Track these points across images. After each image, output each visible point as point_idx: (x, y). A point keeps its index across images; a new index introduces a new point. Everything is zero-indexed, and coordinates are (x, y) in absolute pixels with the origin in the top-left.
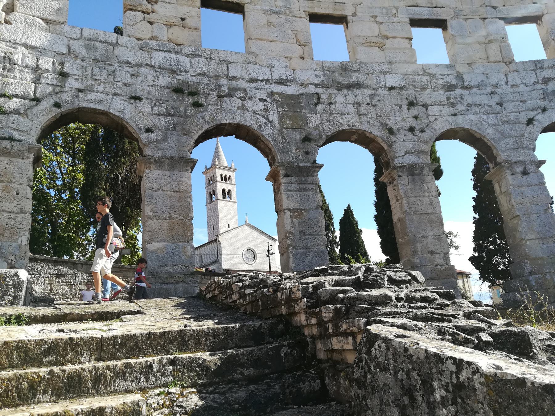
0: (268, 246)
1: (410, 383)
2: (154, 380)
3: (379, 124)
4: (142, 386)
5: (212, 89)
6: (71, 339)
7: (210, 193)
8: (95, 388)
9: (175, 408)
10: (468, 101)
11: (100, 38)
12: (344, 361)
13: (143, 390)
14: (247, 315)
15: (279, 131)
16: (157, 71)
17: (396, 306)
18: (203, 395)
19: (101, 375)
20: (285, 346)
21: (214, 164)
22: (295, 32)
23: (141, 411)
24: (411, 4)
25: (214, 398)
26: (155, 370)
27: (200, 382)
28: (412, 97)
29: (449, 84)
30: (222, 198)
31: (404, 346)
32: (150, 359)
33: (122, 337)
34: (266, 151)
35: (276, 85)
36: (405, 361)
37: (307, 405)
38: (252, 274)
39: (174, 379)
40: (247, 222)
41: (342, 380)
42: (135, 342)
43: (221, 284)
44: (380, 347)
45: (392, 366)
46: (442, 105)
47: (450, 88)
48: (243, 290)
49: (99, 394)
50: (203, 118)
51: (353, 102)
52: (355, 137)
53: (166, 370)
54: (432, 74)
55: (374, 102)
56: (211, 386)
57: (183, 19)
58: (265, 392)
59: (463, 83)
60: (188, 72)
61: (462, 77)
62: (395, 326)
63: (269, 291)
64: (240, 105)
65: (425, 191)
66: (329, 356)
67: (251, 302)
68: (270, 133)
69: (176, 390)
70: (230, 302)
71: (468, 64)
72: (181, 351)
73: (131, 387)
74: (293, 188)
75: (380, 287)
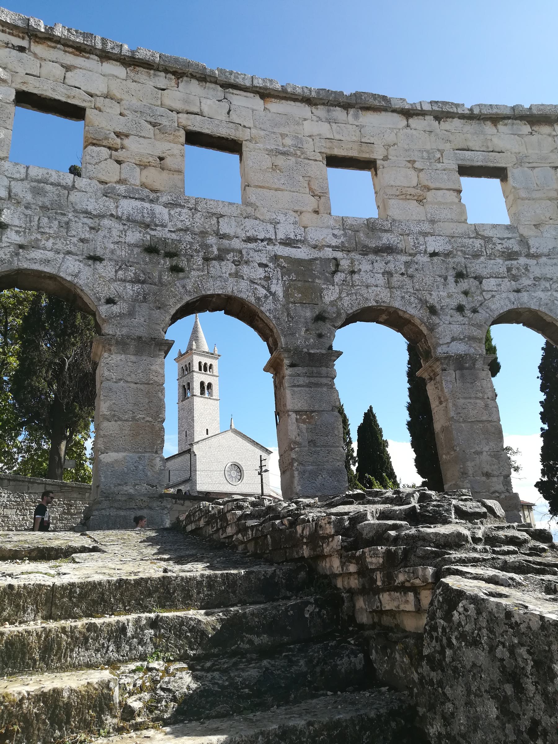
0: (261, 461)
1: (516, 665)
2: (128, 649)
3: (416, 301)
4: (110, 658)
5: (196, 249)
6: (11, 587)
7: (184, 386)
8: (44, 660)
9: (159, 692)
11: (52, 180)
12: (398, 628)
13: (112, 665)
14: (249, 556)
15: (284, 306)
16: (125, 224)
17: (475, 550)
18: (197, 673)
19: (53, 640)
20: (311, 603)
21: (190, 349)
22: (308, 179)
23: (112, 696)
24: (460, 147)
25: (213, 678)
26: (129, 634)
27: (192, 653)
28: (461, 266)
29: (510, 251)
30: (199, 394)
31: (505, 609)
32: (123, 618)
33: (82, 586)
35: (282, 247)
36: (507, 631)
37: (346, 691)
38: (253, 499)
39: (156, 648)
40: (233, 427)
41: (397, 656)
42: (100, 593)
43: (210, 512)
44: (466, 610)
45: (485, 638)
46: (501, 278)
47: (510, 255)
48: (243, 521)
49: (50, 669)
50: (184, 287)
51: (382, 271)
53: (144, 635)
54: (487, 237)
55: (410, 271)
56: (208, 660)
57: (161, 159)
58: (286, 670)
59: (529, 250)
60: (166, 226)
61: (527, 242)
62: (481, 579)
64: (233, 271)
65: (477, 391)
66: (376, 620)
67: (255, 539)
68: (272, 308)
69: (159, 664)
70: (222, 537)
71: (534, 225)
72: (163, 607)
73: (95, 660)
74: (301, 383)
75: (445, 521)
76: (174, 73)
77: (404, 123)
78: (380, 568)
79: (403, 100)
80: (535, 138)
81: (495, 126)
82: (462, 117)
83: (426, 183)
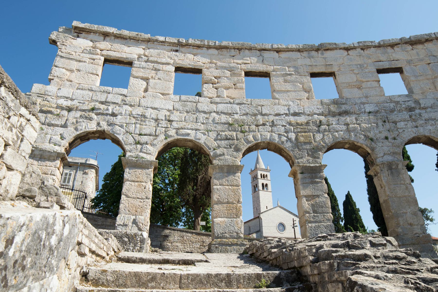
0: (293, 221)
7: (254, 186)
10: (425, 117)
20: (296, 288)
21: (256, 168)
24: (376, 61)
28: (385, 117)
34: (288, 158)
38: (277, 239)
40: (279, 205)
43: (257, 245)
46: (407, 121)
47: (411, 109)
51: (344, 123)
52: (347, 146)
61: (418, 102)
63: (286, 250)
71: (421, 93)
74: (307, 181)
76: (238, 49)
77: (346, 53)
78: (327, 271)
79: (344, 44)
80: (414, 51)
81: (393, 48)
82: (375, 47)
83: (360, 79)
